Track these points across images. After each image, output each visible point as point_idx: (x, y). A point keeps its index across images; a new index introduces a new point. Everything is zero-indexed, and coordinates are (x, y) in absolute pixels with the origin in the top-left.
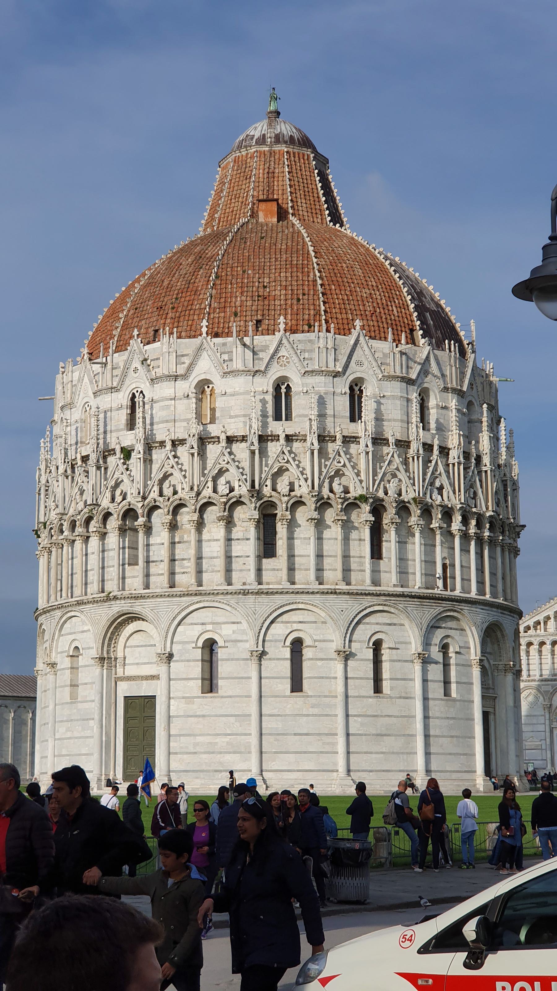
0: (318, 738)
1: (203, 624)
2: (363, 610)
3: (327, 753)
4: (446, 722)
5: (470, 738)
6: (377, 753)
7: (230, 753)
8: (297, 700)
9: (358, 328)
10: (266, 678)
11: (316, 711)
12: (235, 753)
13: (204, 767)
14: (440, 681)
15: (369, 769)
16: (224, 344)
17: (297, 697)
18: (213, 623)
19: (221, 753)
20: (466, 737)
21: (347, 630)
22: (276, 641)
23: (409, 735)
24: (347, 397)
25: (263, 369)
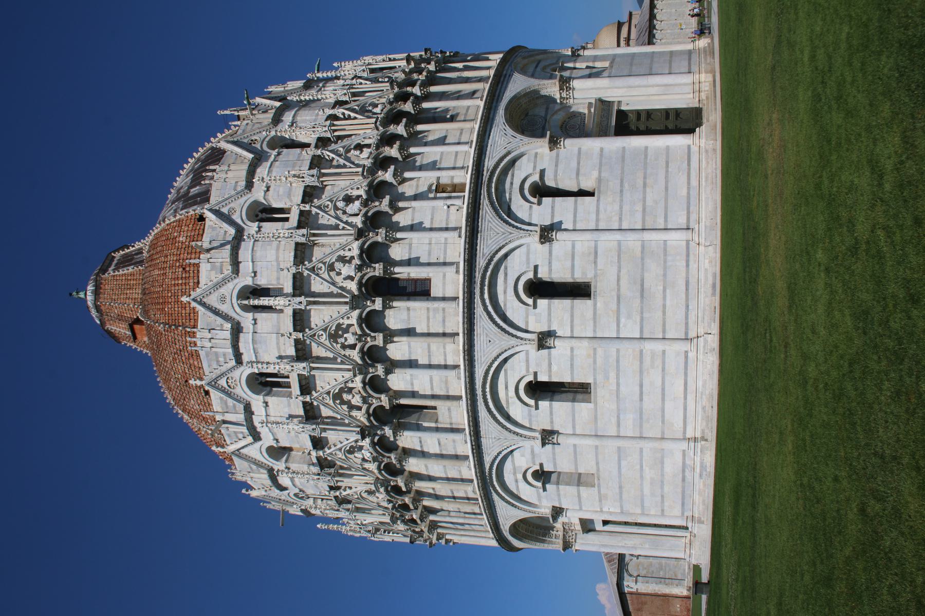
0: (645, 374)
1: (517, 481)
2: (489, 314)
3: (664, 363)
4: (627, 195)
5: (646, 156)
6: (664, 298)
7: (663, 467)
8: (601, 393)
9: (188, 299)
10: (574, 427)
11: (612, 375)
12: (662, 463)
13: (679, 490)
14: (576, 202)
15: (684, 310)
16: (229, 435)
17: (596, 397)
18: (515, 474)
19: (662, 475)
20: (645, 164)
21: (513, 336)
22: (530, 415)
23: (642, 252)
24: (259, 316)
25: (242, 406)
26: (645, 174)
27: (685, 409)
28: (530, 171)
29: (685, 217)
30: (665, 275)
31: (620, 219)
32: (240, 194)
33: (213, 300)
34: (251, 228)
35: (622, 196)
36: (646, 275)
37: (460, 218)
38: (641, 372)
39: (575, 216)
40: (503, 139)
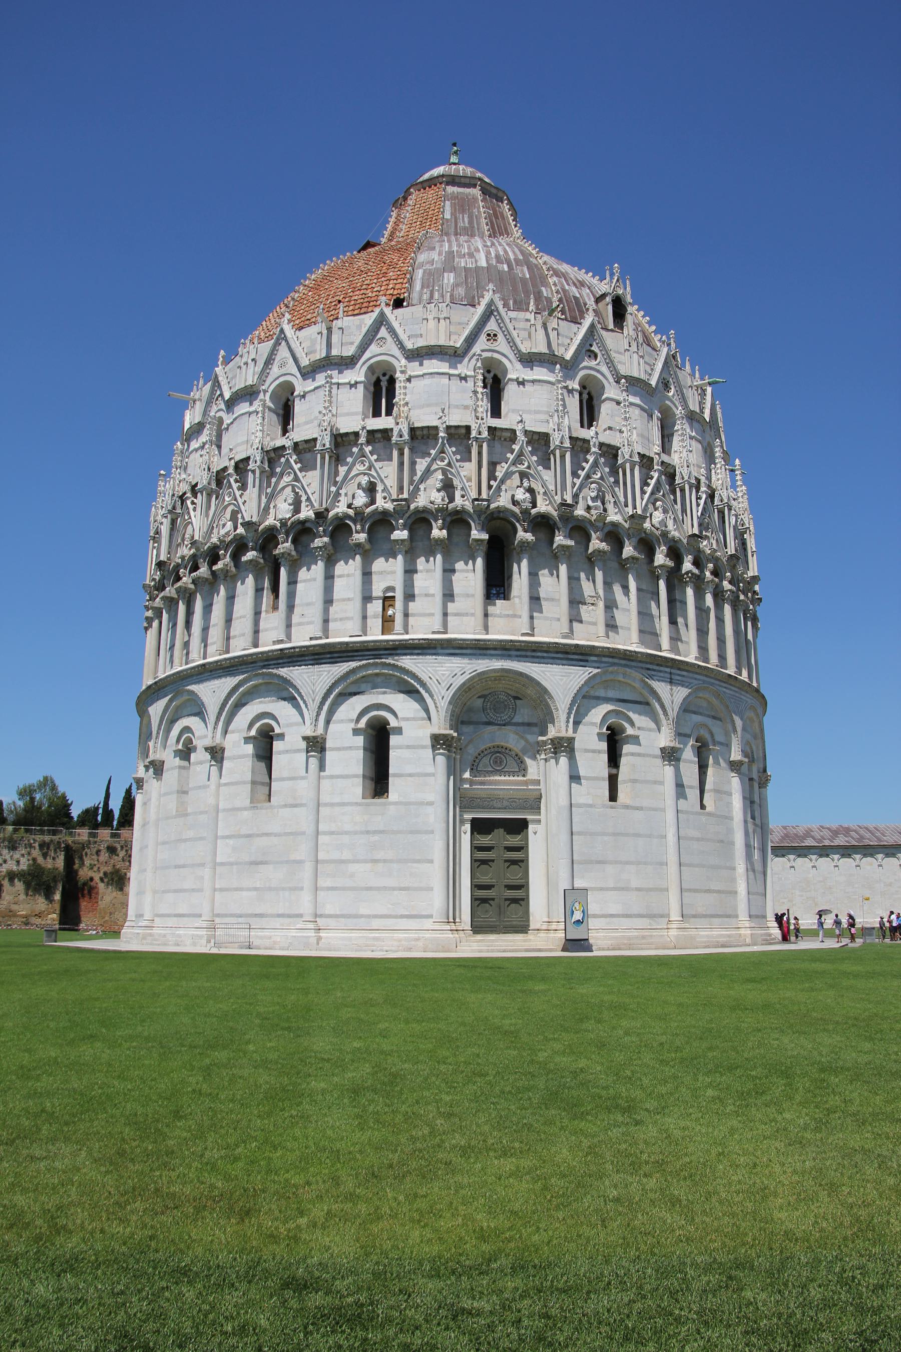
6: (249, 889)
14: (356, 776)
15: (238, 912)
26: (391, 861)
27: (168, 916)
28: (400, 715)
29: (332, 913)
30: (270, 889)
31: (332, 833)
32: (402, 347)
33: (283, 352)
34: (358, 374)
35: (362, 833)
36: (271, 867)
37: (343, 632)
38: (193, 866)
39: (338, 777)
40: (444, 676)
